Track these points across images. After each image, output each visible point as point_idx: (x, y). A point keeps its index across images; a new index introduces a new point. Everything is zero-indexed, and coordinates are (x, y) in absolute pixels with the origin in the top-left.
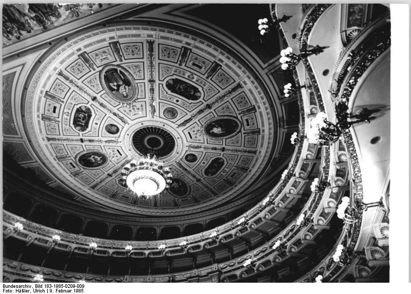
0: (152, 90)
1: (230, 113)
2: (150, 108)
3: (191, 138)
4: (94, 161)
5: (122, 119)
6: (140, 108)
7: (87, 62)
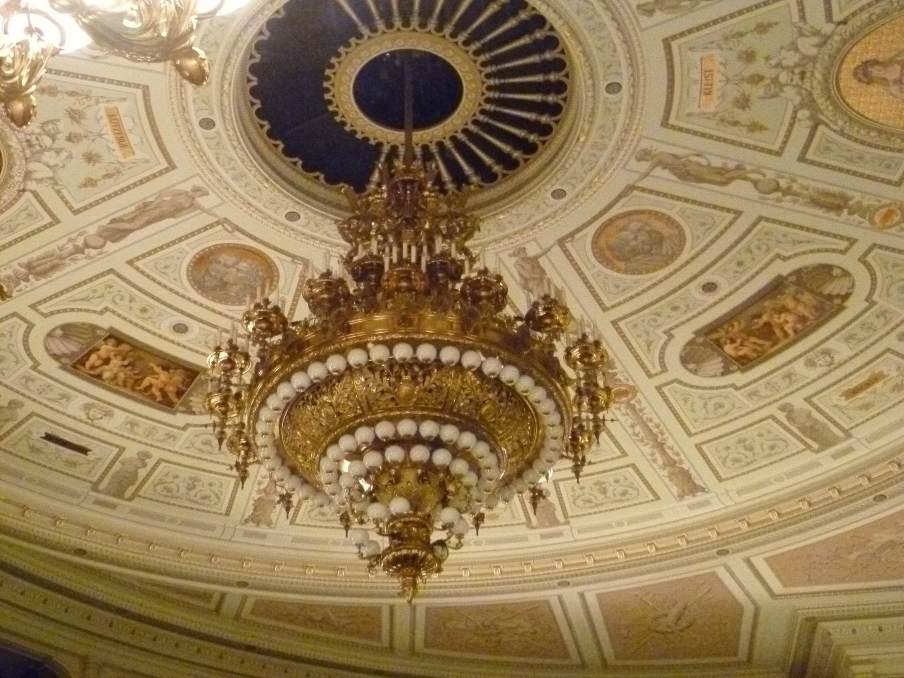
2: (717, 163)
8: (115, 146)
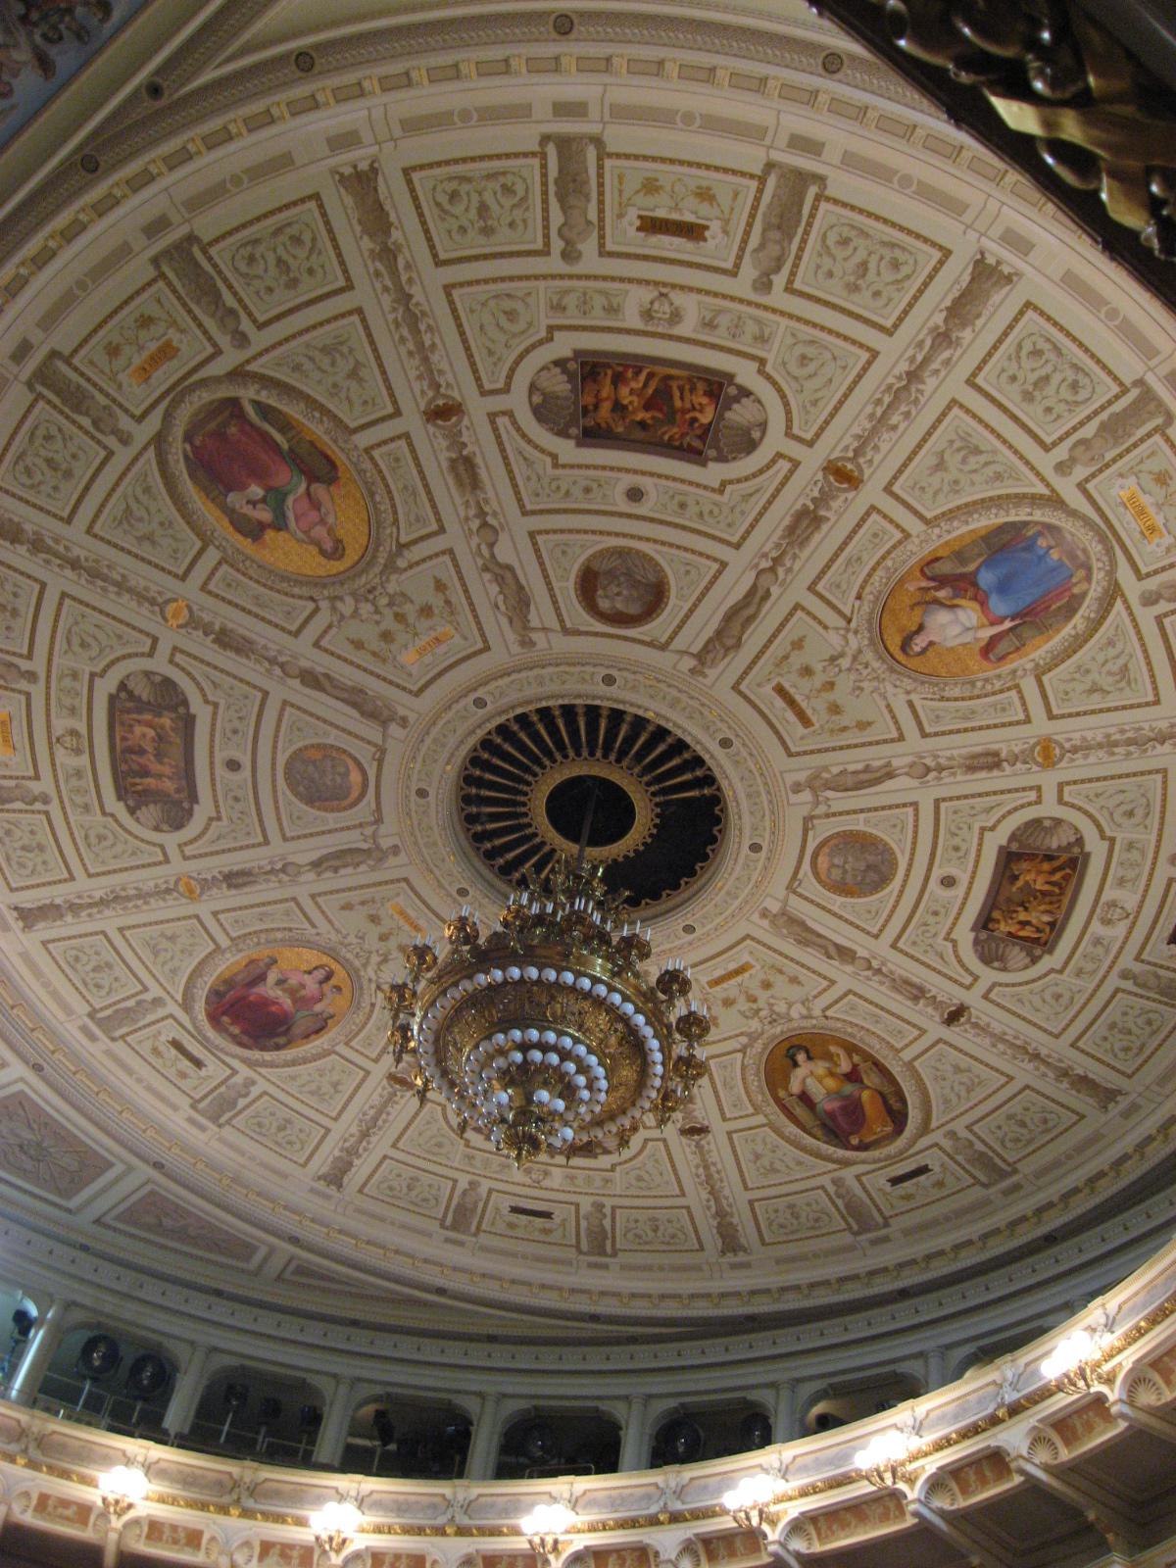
0: (465, 470)
1: (998, 477)
2: (494, 589)
3: (806, 721)
4: (287, 1002)
5: (356, 698)
6: (437, 602)
7: (77, 409)
8: (746, 975)
